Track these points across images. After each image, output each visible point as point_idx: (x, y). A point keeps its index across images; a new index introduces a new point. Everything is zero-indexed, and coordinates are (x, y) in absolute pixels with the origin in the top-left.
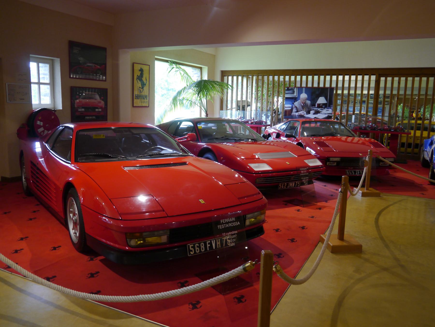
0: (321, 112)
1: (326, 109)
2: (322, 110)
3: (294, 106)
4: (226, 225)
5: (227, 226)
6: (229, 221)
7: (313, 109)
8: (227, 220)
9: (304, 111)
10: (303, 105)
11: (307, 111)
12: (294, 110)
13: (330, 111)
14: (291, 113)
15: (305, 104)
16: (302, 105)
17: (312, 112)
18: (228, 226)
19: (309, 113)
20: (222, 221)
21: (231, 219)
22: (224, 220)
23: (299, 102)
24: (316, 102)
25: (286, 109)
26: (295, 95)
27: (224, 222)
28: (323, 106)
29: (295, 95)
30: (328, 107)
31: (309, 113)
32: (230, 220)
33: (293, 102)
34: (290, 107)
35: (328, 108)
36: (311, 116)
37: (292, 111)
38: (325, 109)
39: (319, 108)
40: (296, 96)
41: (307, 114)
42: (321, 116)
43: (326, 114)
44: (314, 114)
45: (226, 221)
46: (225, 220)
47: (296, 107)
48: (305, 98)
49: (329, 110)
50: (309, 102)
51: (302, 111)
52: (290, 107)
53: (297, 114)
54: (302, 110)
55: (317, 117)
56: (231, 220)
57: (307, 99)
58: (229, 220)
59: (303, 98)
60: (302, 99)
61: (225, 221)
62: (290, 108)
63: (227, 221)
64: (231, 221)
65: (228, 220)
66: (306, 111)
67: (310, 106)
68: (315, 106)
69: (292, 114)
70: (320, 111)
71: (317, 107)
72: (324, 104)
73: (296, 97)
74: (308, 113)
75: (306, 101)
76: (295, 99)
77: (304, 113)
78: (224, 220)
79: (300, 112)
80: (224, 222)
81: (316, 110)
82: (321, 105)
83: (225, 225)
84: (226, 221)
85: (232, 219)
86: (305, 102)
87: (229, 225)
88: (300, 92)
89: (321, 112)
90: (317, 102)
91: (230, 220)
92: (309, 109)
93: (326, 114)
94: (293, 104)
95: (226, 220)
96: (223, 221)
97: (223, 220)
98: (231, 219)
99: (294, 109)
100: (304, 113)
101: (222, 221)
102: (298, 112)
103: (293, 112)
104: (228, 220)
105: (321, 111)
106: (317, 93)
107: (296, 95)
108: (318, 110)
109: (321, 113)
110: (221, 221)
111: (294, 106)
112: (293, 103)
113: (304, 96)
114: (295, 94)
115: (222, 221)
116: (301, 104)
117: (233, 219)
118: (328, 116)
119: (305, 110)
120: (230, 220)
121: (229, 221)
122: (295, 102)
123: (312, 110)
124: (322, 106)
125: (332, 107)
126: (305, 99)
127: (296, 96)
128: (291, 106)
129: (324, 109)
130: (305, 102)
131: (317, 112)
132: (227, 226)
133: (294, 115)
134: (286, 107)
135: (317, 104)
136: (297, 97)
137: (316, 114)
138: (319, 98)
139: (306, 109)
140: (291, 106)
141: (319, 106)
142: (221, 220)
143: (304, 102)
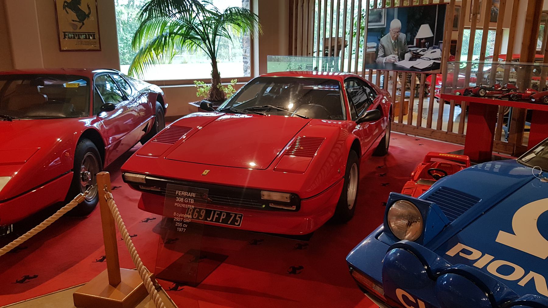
0: (422, 55)
1: (430, 50)
2: (424, 51)
3: (380, 45)
6: (186, 195)
7: (410, 50)
9: (395, 54)
10: (395, 42)
11: (399, 54)
12: (381, 53)
13: (438, 53)
14: (376, 59)
15: (396, 41)
16: (393, 42)
17: (408, 56)
19: (403, 59)
20: (178, 192)
21: (190, 193)
22: (180, 192)
23: (387, 36)
24: (415, 36)
25: (368, 50)
26: (382, 23)
27: (180, 194)
28: (426, 44)
29: (382, 23)
30: (434, 46)
31: (403, 58)
32: (188, 194)
33: (379, 38)
34: (374, 47)
35: (434, 48)
36: (406, 64)
37: (377, 55)
38: (429, 50)
39: (420, 47)
40: (384, 25)
41: (399, 61)
42: (421, 64)
43: (430, 59)
44: (411, 60)
45: (182, 194)
46: (181, 193)
47: (383, 47)
48: (396, 29)
49: (436, 51)
50: (403, 36)
51: (391, 54)
52: (374, 47)
53: (384, 60)
54: (392, 53)
55: (414, 66)
57: (401, 30)
58: (187, 194)
59: (395, 29)
60: (392, 30)
62: (374, 50)
63: (184, 194)
64: (189, 196)
65: (186, 193)
66: (398, 54)
67: (405, 44)
68: (413, 44)
69: (377, 61)
70: (420, 53)
71: (416, 47)
72: (427, 39)
73: (384, 28)
74: (402, 58)
75: (399, 34)
76: (382, 32)
77: (394, 57)
78: (180, 192)
79: (388, 56)
80: (180, 194)
81: (414, 52)
82: (422, 41)
84: (183, 195)
85: (192, 195)
86: (398, 36)
88: (390, 19)
89: (422, 55)
90: (416, 35)
91: (189, 195)
92: (402, 51)
93: (430, 59)
94: (379, 41)
95: (183, 193)
96: (179, 193)
97: (180, 192)
98: (190, 193)
99: (379, 52)
100: (394, 57)
101: (177, 192)
102: (386, 57)
103: (379, 56)
104: (186, 194)
105: (422, 53)
106: (418, 16)
107: (383, 24)
108: (418, 51)
109: (422, 57)
111: (381, 44)
112: (379, 40)
113: (396, 24)
114: (383, 22)
115: (177, 192)
116: (391, 41)
117: (193, 195)
118: (434, 63)
119: (397, 52)
120: (188, 194)
121: (186, 195)
122: (382, 37)
123: (407, 52)
124: (425, 43)
125: (441, 45)
126: (398, 30)
127: (384, 25)
128: (375, 44)
129: (428, 48)
130: (398, 36)
131: (416, 57)
133: (380, 62)
134: (369, 48)
135: (417, 39)
136: (385, 26)
137: (414, 59)
138: (420, 26)
139: (398, 51)
140: (375, 44)
141: (421, 44)
142: (177, 191)
143: (396, 36)
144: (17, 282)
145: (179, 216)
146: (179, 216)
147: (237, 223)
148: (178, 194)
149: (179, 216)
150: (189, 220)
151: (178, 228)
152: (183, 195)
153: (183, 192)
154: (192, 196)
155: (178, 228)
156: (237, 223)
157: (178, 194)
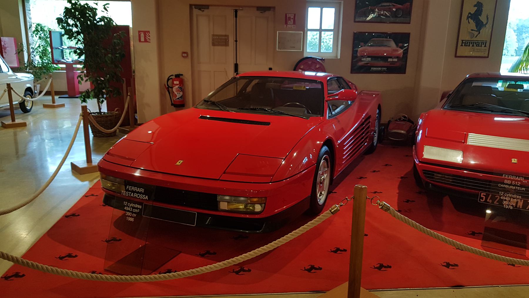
4: (131, 194)
5: (132, 195)
6: (136, 190)
8: (134, 189)
18: (133, 195)
21: (139, 188)
22: (130, 187)
27: (130, 189)
32: (137, 190)
45: (132, 189)
46: (131, 188)
56: (139, 190)
58: (136, 189)
61: (131, 189)
63: (134, 189)
64: (138, 191)
65: (136, 188)
78: (130, 187)
80: (130, 189)
83: (130, 193)
84: (133, 190)
85: (141, 190)
87: (135, 195)
91: (138, 190)
95: (133, 188)
96: (130, 188)
98: (139, 188)
101: (128, 187)
104: (135, 189)
110: (127, 187)
115: (128, 187)
117: (142, 190)
120: (137, 190)
121: (136, 190)
132: (132, 195)
144: (200, 255)
145: (130, 206)
146: (130, 206)
147: (483, 200)
148: (128, 189)
149: (130, 206)
150: (138, 210)
151: (127, 217)
152: (133, 190)
153: (133, 187)
154: (141, 191)
155: (127, 217)
156: (483, 200)
157: (128, 189)
